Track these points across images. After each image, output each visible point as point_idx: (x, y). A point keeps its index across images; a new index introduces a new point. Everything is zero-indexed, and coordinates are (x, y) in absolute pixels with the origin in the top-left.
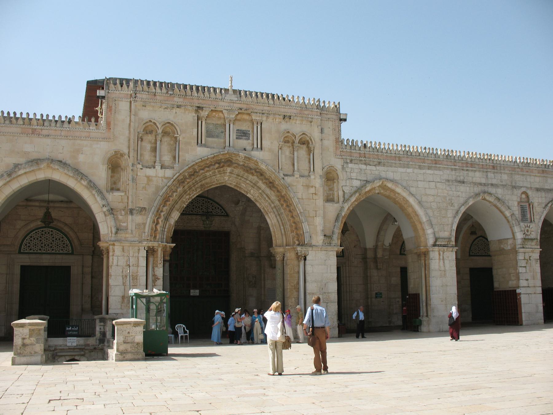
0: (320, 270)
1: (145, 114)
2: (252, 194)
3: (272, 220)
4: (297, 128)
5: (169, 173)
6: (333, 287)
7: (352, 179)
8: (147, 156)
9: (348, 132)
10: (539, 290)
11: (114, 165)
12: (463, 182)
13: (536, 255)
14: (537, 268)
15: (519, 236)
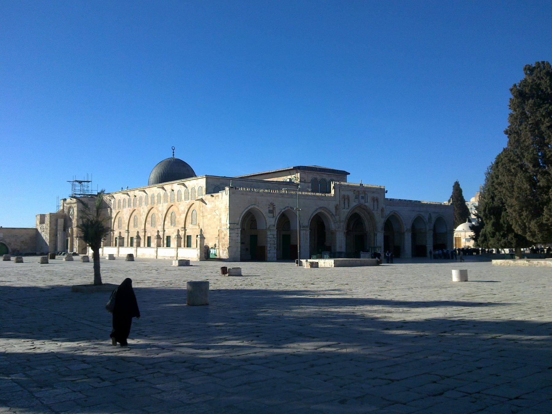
0: (380, 239)
1: (343, 193)
2: (362, 215)
3: (366, 223)
4: (375, 195)
5: (348, 210)
6: (383, 244)
7: (388, 211)
8: (343, 206)
9: (387, 196)
10: (432, 246)
11: (337, 208)
12: (414, 211)
13: (432, 234)
14: (432, 238)
15: (428, 228)
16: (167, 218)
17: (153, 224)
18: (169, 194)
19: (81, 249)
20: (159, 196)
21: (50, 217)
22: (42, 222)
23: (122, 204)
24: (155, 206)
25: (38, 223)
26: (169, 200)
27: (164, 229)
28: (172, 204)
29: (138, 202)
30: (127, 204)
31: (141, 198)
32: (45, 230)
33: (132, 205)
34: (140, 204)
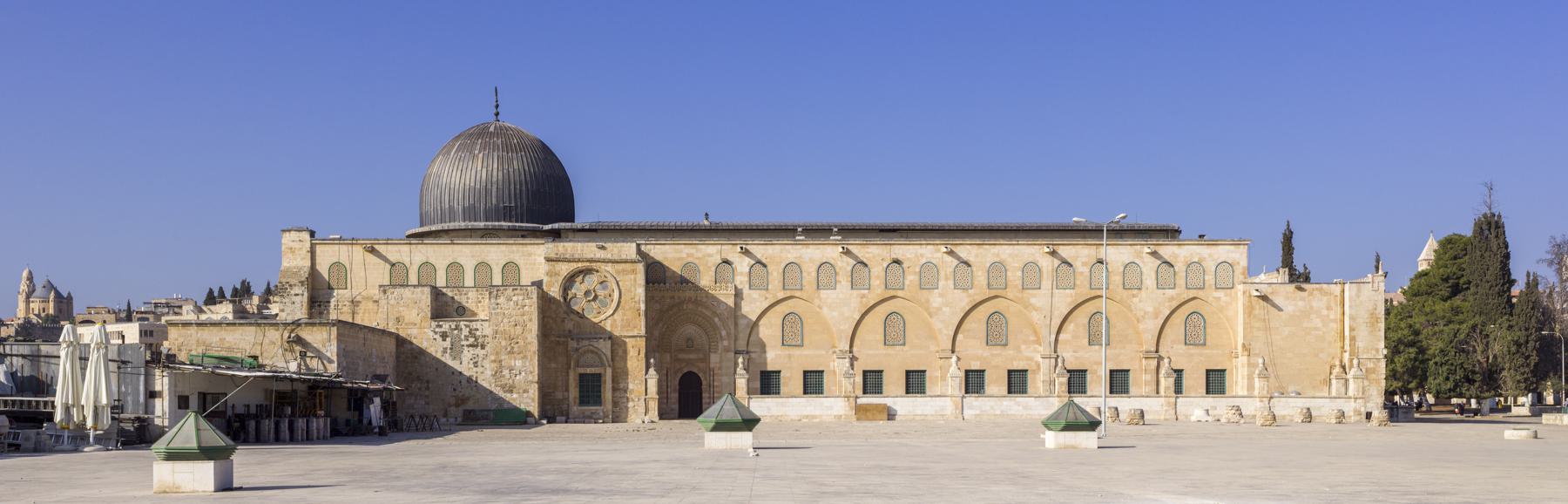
16: (1070, 327)
20: (1030, 267)
24: (1010, 293)
29: (911, 278)
31: (928, 268)
33: (877, 283)
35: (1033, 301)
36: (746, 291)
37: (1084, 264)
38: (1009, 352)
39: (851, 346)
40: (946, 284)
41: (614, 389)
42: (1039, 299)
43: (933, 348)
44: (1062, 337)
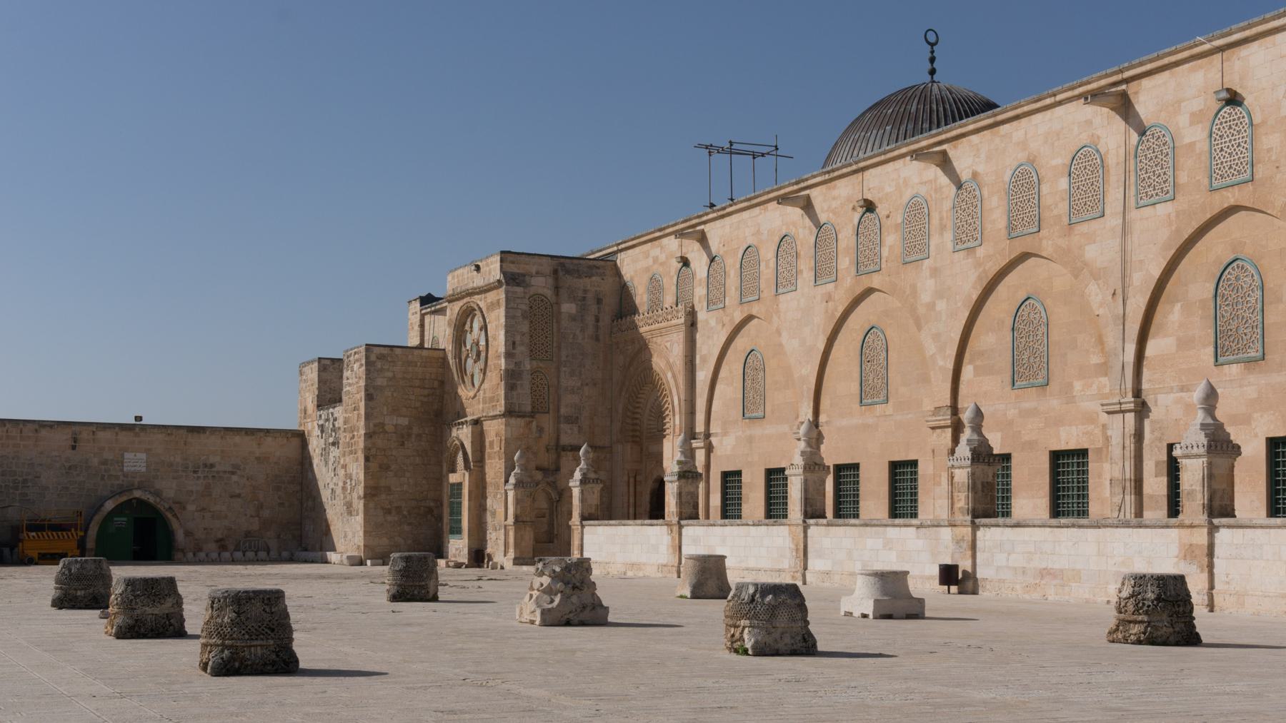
16: (1171, 315)
17: (1030, 367)
18: (1193, 135)
19: (529, 535)
20: (1085, 164)
21: (369, 363)
22: (329, 396)
23: (767, 271)
24: (1048, 242)
25: (310, 400)
26: (1191, 172)
27: (1137, 393)
28: (1231, 197)
29: (892, 240)
30: (806, 266)
31: (917, 211)
32: (344, 438)
33: (845, 263)
34: (915, 250)
35: (1091, 253)
36: (702, 316)
37: (1195, 118)
38: (1053, 403)
39: (816, 412)
40: (941, 241)
41: (452, 514)
42: (1099, 246)
43: (928, 406)
44: (1152, 348)
